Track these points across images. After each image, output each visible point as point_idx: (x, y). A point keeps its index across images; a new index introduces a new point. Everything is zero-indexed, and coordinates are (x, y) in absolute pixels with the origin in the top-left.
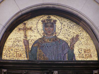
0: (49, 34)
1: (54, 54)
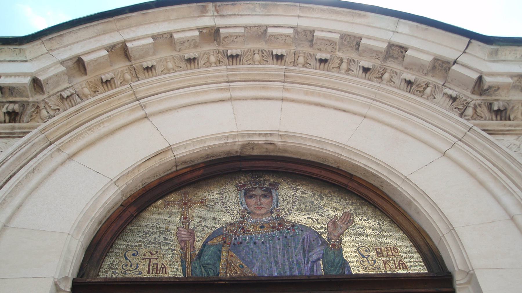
0: (259, 212)
1: (277, 263)
